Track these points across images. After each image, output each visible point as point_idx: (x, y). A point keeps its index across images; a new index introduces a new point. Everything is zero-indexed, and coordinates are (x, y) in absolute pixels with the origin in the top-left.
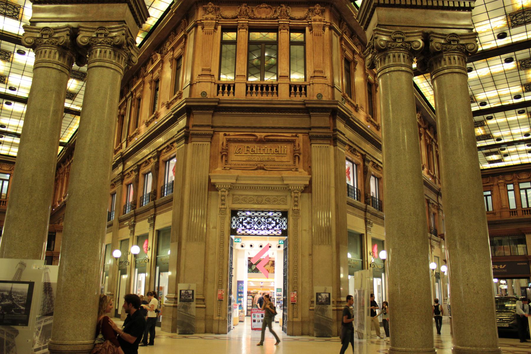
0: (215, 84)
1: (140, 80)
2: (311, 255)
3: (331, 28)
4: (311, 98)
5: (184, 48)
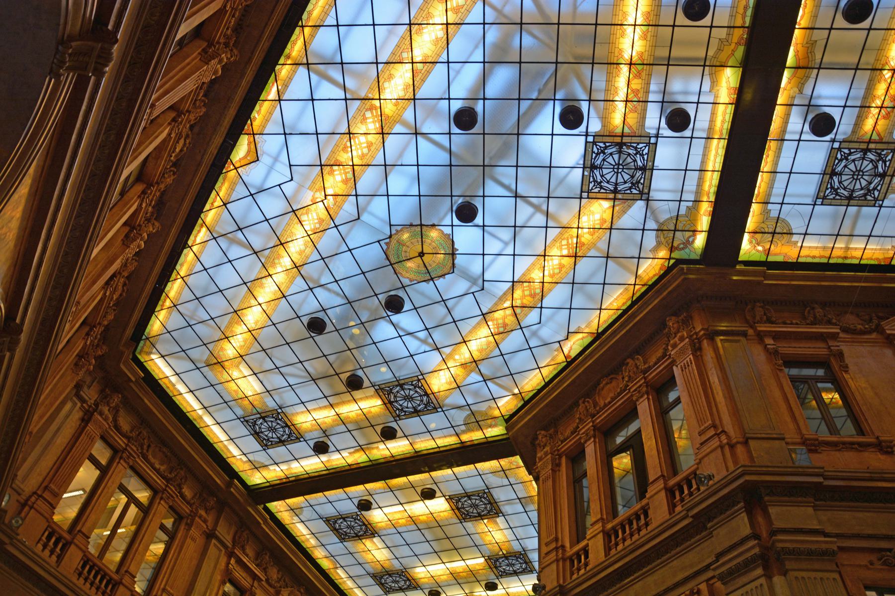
0: (564, 560)
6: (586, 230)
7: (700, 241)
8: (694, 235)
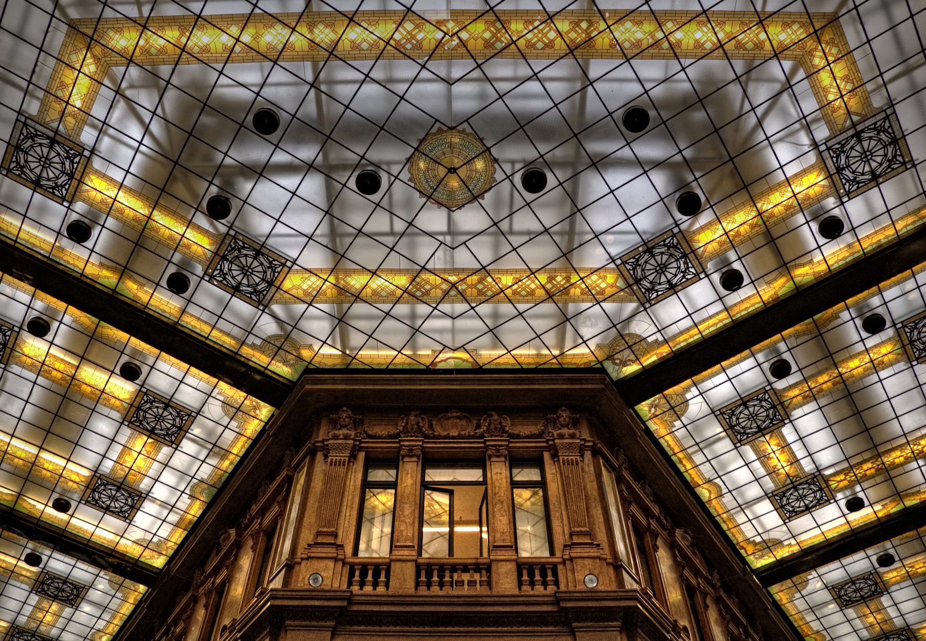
0: (344, 563)
1: (190, 594)
3: (596, 453)
4: (571, 588)
5: (285, 500)
6: (583, 286)
7: (632, 369)
8: (633, 362)
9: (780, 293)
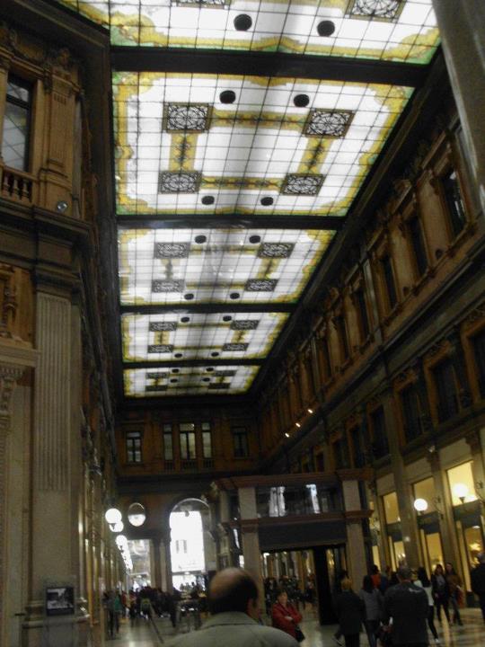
2: (30, 511)
4: (41, 205)
9: (264, 50)
